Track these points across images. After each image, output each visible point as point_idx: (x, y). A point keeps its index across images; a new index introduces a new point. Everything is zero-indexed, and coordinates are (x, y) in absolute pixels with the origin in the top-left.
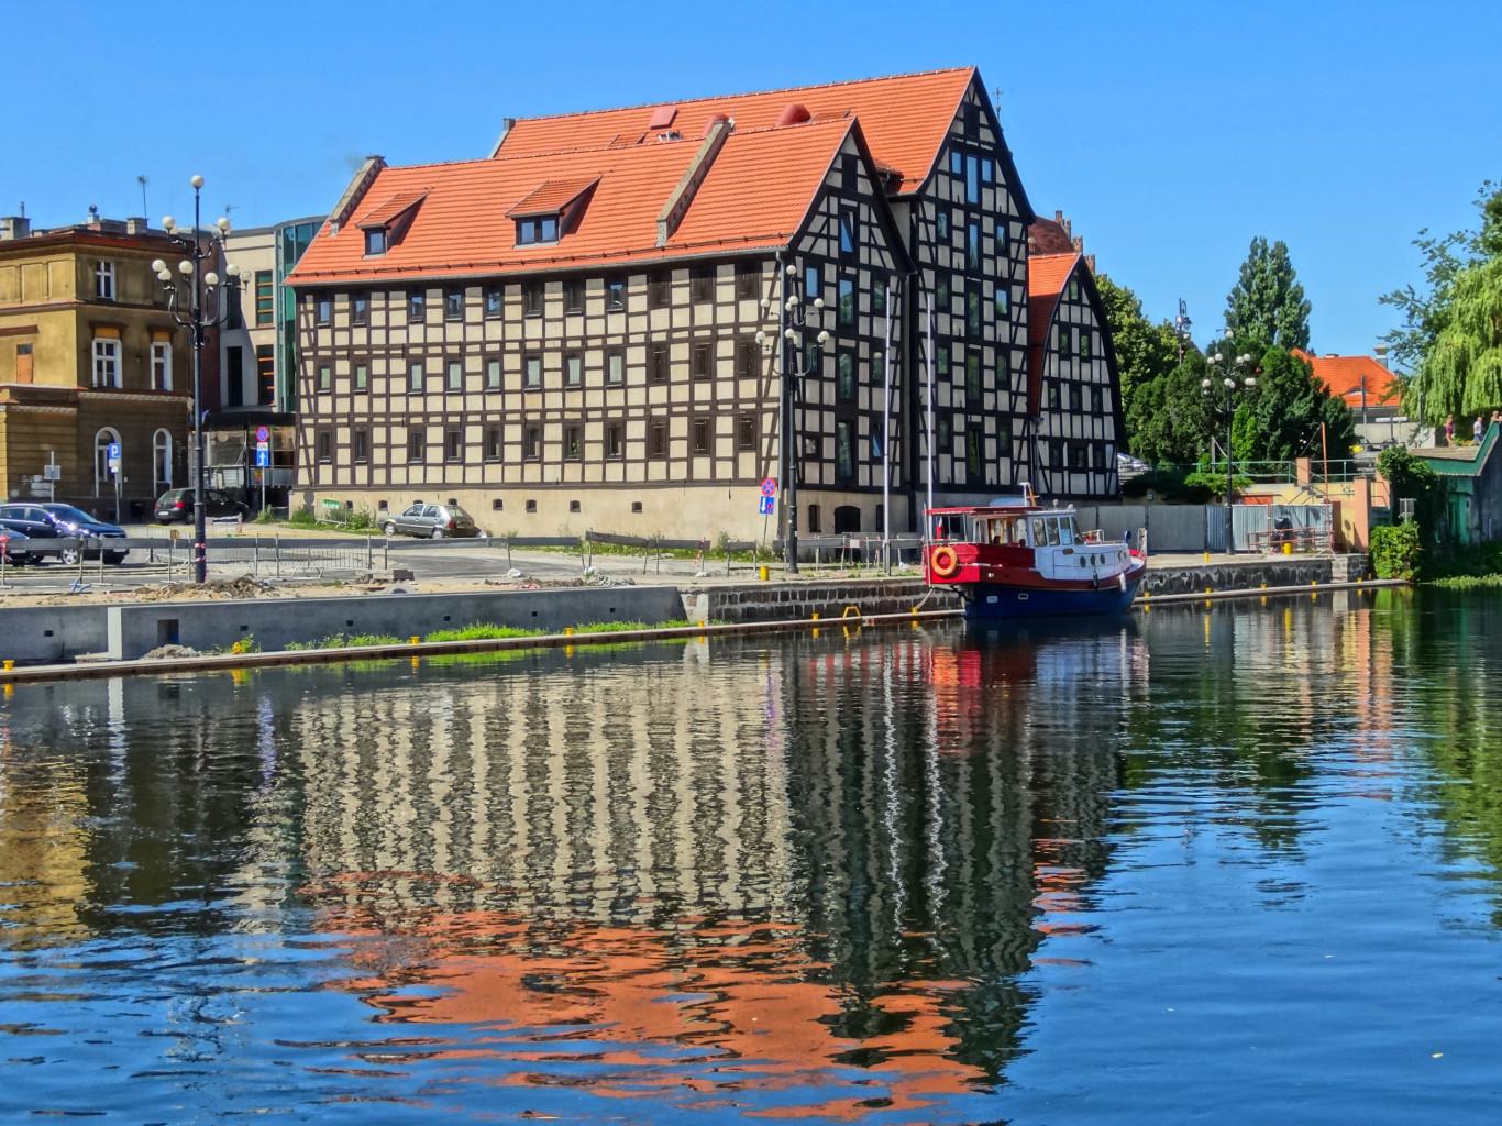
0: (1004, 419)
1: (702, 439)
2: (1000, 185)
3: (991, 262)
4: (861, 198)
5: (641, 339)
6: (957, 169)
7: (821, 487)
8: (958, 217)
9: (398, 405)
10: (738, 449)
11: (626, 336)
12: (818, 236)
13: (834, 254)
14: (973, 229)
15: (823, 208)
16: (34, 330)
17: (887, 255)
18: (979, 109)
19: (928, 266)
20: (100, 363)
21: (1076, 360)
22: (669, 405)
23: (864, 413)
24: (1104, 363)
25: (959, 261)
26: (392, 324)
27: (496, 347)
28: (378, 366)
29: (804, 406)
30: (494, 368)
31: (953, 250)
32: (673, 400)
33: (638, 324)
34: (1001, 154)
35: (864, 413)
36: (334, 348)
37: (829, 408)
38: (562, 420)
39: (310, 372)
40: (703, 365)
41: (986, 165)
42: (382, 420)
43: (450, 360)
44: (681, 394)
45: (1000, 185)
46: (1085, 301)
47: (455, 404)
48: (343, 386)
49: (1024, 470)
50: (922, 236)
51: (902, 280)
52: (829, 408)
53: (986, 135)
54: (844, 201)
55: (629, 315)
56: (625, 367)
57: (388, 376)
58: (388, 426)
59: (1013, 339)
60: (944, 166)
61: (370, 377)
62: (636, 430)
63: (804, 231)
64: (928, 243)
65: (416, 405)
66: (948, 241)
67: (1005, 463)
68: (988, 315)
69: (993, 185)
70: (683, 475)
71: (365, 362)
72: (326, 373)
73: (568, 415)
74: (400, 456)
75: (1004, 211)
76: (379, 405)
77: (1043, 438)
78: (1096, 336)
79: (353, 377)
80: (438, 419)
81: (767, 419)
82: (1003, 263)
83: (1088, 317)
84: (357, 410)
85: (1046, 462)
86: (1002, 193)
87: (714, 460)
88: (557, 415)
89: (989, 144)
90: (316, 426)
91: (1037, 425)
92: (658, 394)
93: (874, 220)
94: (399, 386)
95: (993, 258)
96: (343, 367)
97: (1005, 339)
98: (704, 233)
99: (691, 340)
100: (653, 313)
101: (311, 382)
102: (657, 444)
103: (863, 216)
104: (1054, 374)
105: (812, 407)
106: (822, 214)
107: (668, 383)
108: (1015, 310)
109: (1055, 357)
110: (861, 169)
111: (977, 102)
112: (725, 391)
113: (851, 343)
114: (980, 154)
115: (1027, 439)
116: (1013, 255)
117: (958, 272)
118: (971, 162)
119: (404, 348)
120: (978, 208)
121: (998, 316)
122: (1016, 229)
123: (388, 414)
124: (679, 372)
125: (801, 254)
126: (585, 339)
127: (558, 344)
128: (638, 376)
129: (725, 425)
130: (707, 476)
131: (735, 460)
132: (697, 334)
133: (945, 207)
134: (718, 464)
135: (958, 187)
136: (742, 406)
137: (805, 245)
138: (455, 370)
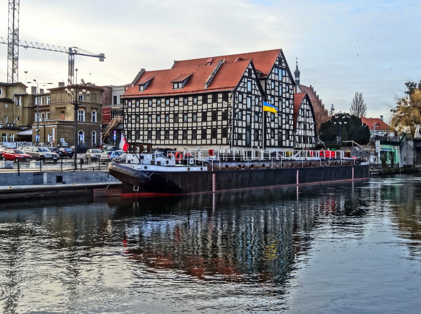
0: (287, 131)
1: (214, 135)
2: (287, 76)
3: (285, 94)
4: (253, 79)
5: (201, 111)
6: (276, 72)
7: (242, 146)
8: (277, 84)
9: (146, 126)
10: (223, 137)
11: (197, 110)
12: (242, 87)
13: (246, 92)
14: (280, 86)
15: (243, 81)
16: (65, 107)
17: (259, 92)
18: (282, 59)
19: (269, 95)
20: (80, 115)
22: (207, 126)
24: (312, 118)
25: (277, 94)
26: (145, 107)
27: (168, 113)
28: (141, 117)
29: (238, 127)
30: (167, 117)
31: (275, 91)
32: (208, 125)
33: (200, 107)
36: (132, 113)
37: (244, 128)
38: (182, 130)
39: (126, 118)
40: (214, 118)
41: (284, 72)
42: (142, 129)
43: (157, 115)
44: (209, 124)
45: (287, 76)
46: (308, 103)
47: (158, 125)
48: (133, 121)
49: (292, 143)
50: (268, 88)
51: (262, 98)
52: (244, 128)
53: (284, 65)
54: (248, 79)
55: (198, 105)
56: (197, 117)
57: (143, 119)
58: (143, 130)
59: (290, 112)
60: (273, 71)
61: (140, 119)
62: (199, 132)
63: (238, 86)
64: (269, 89)
65: (150, 126)
66: (274, 89)
67: (288, 141)
68: (284, 107)
69: (285, 76)
70: (210, 143)
71: (139, 115)
72: (130, 118)
73: (184, 128)
74: (146, 138)
75: (288, 82)
76: (142, 126)
78: (310, 112)
79: (136, 119)
80: (155, 129)
81: (229, 130)
82: (287, 94)
83: (308, 108)
84: (137, 127)
85: (298, 141)
86: (287, 78)
87: (217, 139)
88: (181, 129)
89: (284, 67)
90: (127, 130)
91: (295, 132)
92: (204, 124)
93: (256, 84)
94: (146, 121)
95: (285, 93)
96: (133, 117)
97: (288, 112)
98: (216, 86)
99: (212, 111)
100: (203, 105)
101: (126, 120)
102: (204, 136)
103: (253, 83)
104: (300, 120)
105: (240, 127)
106: (243, 82)
107: (207, 121)
108: (290, 105)
109: (300, 116)
110: (253, 72)
111: (282, 57)
112: (219, 123)
113: (250, 113)
114: (282, 69)
115: (293, 135)
116: (290, 93)
117: (277, 96)
119: (148, 112)
120: (282, 82)
121: (286, 107)
122: (291, 87)
123: (143, 128)
124: (209, 119)
126: (188, 111)
127: (182, 112)
128: (200, 119)
129: (219, 131)
130: (215, 143)
131: (222, 139)
132: (213, 110)
133: (273, 81)
134: (218, 140)
135: (277, 77)
136: (223, 127)
137: (239, 89)
138: (159, 118)
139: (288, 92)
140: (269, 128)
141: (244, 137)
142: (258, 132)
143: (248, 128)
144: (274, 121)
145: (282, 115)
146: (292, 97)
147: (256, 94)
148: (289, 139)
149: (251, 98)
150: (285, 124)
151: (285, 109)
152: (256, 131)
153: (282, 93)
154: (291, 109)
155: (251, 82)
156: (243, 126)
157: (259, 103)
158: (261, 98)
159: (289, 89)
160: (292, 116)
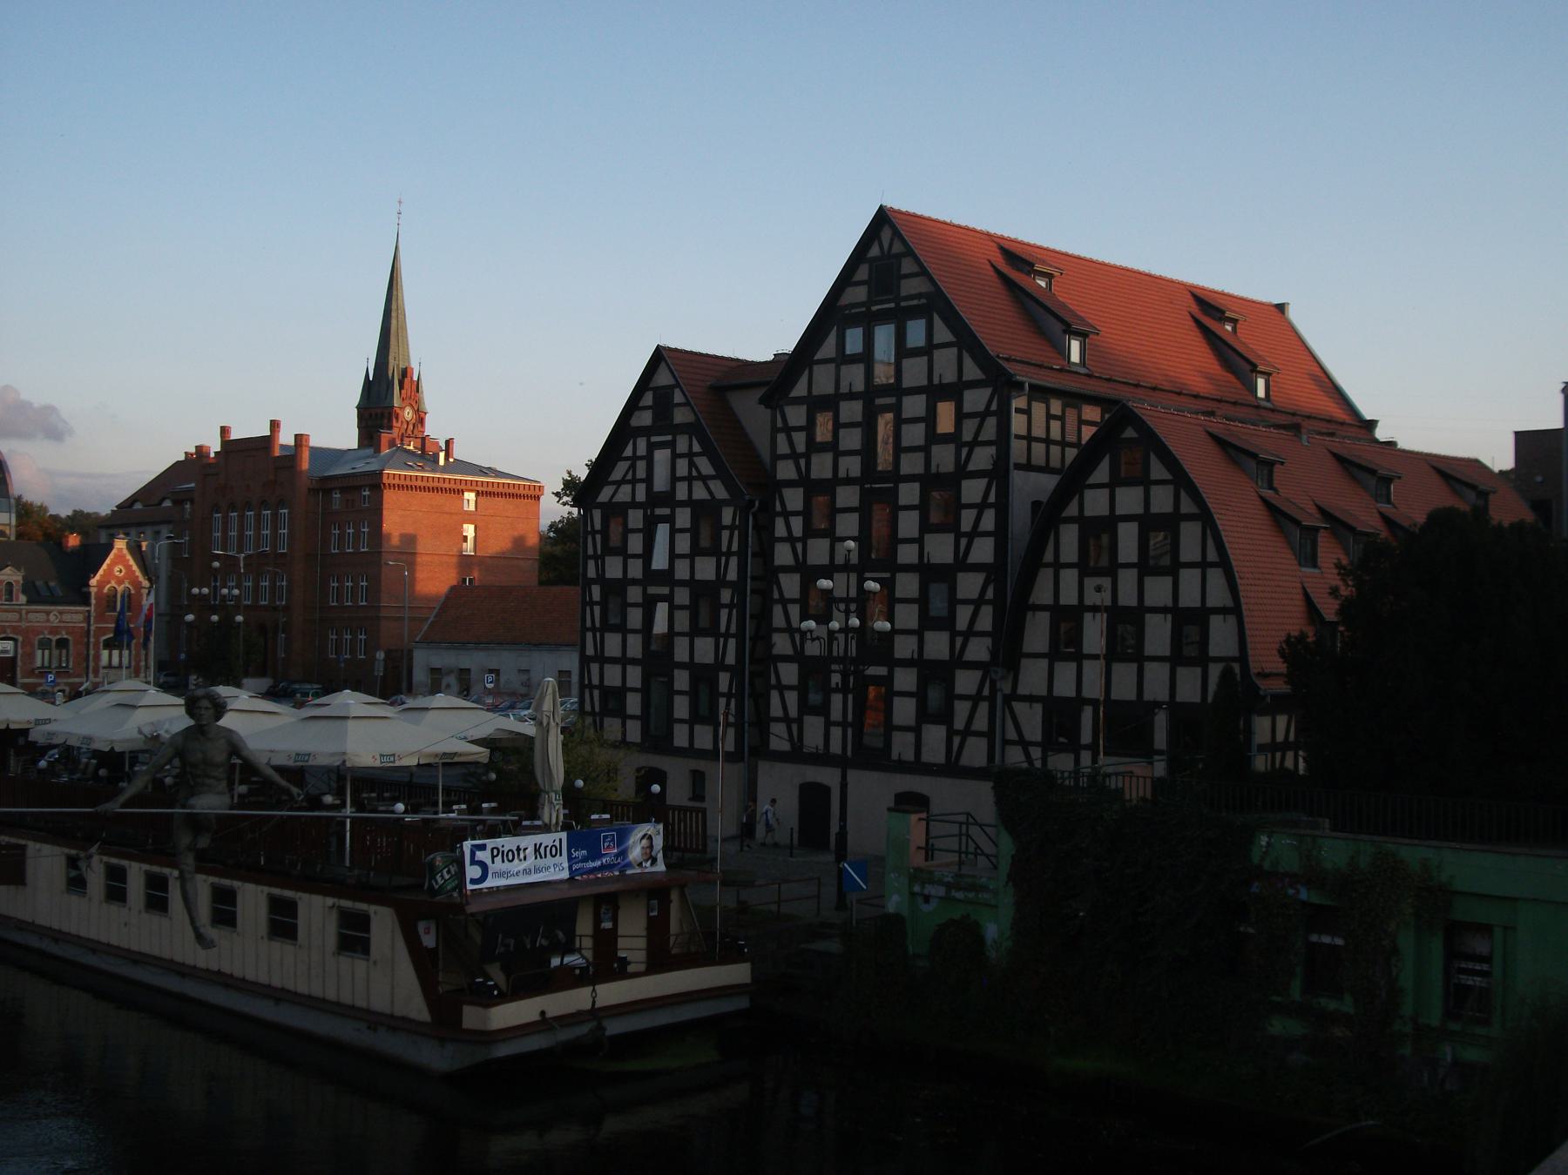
0: (935, 673)
3: (920, 456)
12: (619, 484)
14: (884, 423)
15: (628, 452)
18: (899, 256)
21: (1127, 579)
23: (682, 666)
24: (1216, 577)
29: (602, 660)
34: (936, 305)
35: (682, 666)
37: (634, 662)
46: (1158, 471)
51: (744, 510)
52: (634, 662)
54: (654, 439)
60: (828, 349)
64: (794, 456)
75: (950, 377)
77: (1031, 699)
89: (919, 296)
93: (697, 448)
104: (1069, 597)
105: (613, 661)
109: (1069, 577)
113: (665, 590)
114: (899, 317)
117: (849, 481)
118: (884, 337)
121: (926, 527)
125: (601, 505)
140: (786, 659)
141: (633, 704)
142: (714, 683)
143: (657, 661)
146: (983, 458)
147: (695, 496)
148: (945, 717)
149: (670, 520)
151: (920, 541)
152: (703, 676)
153: (899, 450)
154: (975, 533)
155: (671, 445)
156: (630, 653)
159: (960, 416)
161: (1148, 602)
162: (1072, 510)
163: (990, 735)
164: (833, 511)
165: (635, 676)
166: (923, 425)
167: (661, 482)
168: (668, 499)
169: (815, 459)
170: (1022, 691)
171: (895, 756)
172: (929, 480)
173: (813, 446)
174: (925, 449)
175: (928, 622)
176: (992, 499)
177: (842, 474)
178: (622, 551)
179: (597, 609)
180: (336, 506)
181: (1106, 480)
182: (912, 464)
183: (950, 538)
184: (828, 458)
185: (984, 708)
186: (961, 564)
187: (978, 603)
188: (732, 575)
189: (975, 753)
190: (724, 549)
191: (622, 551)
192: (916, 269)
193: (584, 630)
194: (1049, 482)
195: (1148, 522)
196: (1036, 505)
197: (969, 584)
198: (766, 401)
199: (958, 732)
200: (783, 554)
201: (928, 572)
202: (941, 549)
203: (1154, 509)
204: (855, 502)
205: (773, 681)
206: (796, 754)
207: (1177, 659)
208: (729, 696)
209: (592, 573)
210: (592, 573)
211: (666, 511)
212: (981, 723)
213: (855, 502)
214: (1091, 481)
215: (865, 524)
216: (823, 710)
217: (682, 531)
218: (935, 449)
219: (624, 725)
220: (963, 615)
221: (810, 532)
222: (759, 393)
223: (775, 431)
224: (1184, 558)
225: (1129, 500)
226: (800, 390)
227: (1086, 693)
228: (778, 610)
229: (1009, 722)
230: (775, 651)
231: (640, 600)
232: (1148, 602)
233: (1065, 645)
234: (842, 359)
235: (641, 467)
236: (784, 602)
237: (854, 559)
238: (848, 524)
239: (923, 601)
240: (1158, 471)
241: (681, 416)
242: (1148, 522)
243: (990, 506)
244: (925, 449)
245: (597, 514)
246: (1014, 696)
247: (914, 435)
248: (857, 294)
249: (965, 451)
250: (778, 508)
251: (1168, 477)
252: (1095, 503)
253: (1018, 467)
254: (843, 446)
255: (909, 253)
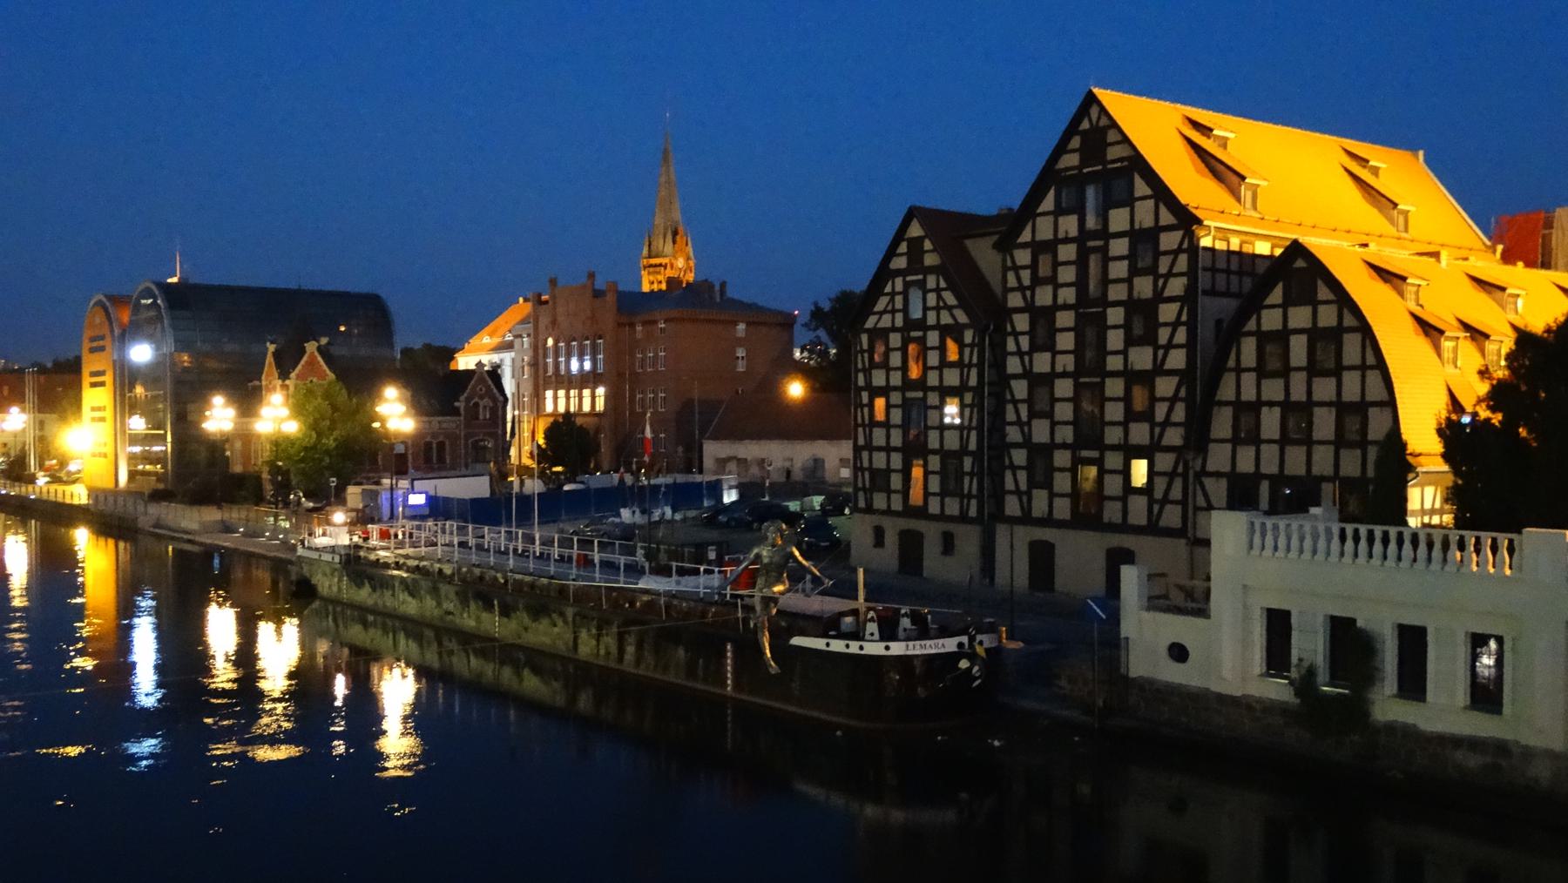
3: (1123, 287)
7: (888, 512)
12: (881, 313)
13: (899, 321)
14: (1094, 262)
15: (888, 289)
18: (1105, 130)
21: (1298, 382)
23: (934, 452)
24: (1373, 377)
29: (870, 447)
34: (1138, 164)
35: (934, 452)
37: (896, 449)
46: (1324, 293)
51: (981, 332)
52: (896, 449)
54: (909, 278)
64: (1021, 288)
77: (1218, 475)
89: (1121, 160)
93: (943, 284)
104: (1249, 394)
105: (880, 449)
109: (1249, 380)
113: (920, 394)
117: (1066, 307)
120: (1105, 234)
121: (1130, 341)
125: (867, 331)
139: (1152, 270)
140: (1017, 445)
141: (896, 481)
144: (1049, 415)
145: (1103, 383)
146: (1176, 286)
149: (922, 341)
150: (1125, 424)
151: (1124, 353)
154: (1170, 346)
157: (961, 353)
158: (968, 336)
160: (1175, 380)
161: (1316, 397)
162: (1251, 325)
163: (1183, 503)
164: (1053, 331)
165: (897, 460)
166: (1126, 263)
167: (916, 314)
168: (922, 325)
169: (1038, 291)
170: (1210, 467)
171: (1106, 520)
172: (1133, 306)
173: (1037, 281)
174: (1129, 281)
175: (1131, 416)
176: (1184, 318)
177: (1060, 301)
178: (885, 366)
179: (866, 410)
180: (639, 336)
181: (1280, 301)
182: (1117, 292)
183: (1149, 351)
184: (1049, 289)
185: (1178, 484)
186: (1159, 370)
187: (1173, 400)
188: (973, 381)
189: (1171, 517)
190: (967, 360)
191: (885, 366)
192: (1119, 138)
193: (857, 425)
194: (1229, 305)
195: (1315, 335)
196: (1219, 322)
197: (1165, 386)
198: (998, 246)
199: (1157, 501)
200: (1013, 366)
201: (1132, 377)
202: (1142, 358)
203: (1321, 324)
204: (1072, 324)
205: (1007, 462)
206: (1026, 519)
207: (1340, 442)
208: (971, 474)
209: (861, 381)
210: (861, 381)
211: (920, 334)
212: (1176, 493)
213: (1072, 324)
214: (1268, 301)
215: (1079, 341)
216: (1048, 484)
217: (932, 348)
218: (1137, 281)
219: (889, 498)
220: (1161, 411)
221: (1034, 348)
222: (996, 237)
223: (1005, 270)
224: (1346, 362)
225: (1300, 317)
226: (1026, 236)
227: (1264, 470)
228: (1010, 407)
229: (1199, 492)
230: (1009, 439)
231: (899, 402)
232: (1316, 397)
233: (1245, 434)
234: (1059, 211)
235: (899, 300)
236: (1015, 402)
237: (1071, 368)
238: (1066, 341)
239: (1127, 399)
240: (1324, 293)
241: (930, 260)
242: (1315, 335)
243: (1183, 324)
244: (1129, 281)
245: (864, 338)
246: (1204, 472)
247: (1119, 269)
248: (1070, 160)
249: (1161, 282)
250: (1009, 329)
251: (1331, 297)
252: (1271, 320)
253: (1205, 293)
254: (1061, 280)
255: (1114, 125)
